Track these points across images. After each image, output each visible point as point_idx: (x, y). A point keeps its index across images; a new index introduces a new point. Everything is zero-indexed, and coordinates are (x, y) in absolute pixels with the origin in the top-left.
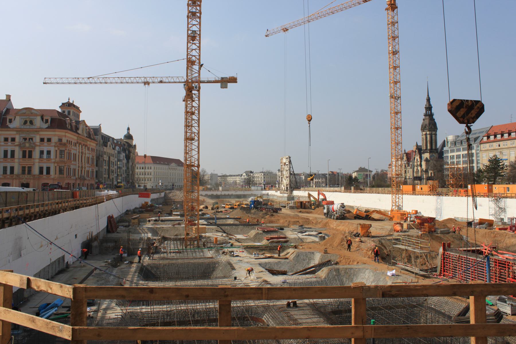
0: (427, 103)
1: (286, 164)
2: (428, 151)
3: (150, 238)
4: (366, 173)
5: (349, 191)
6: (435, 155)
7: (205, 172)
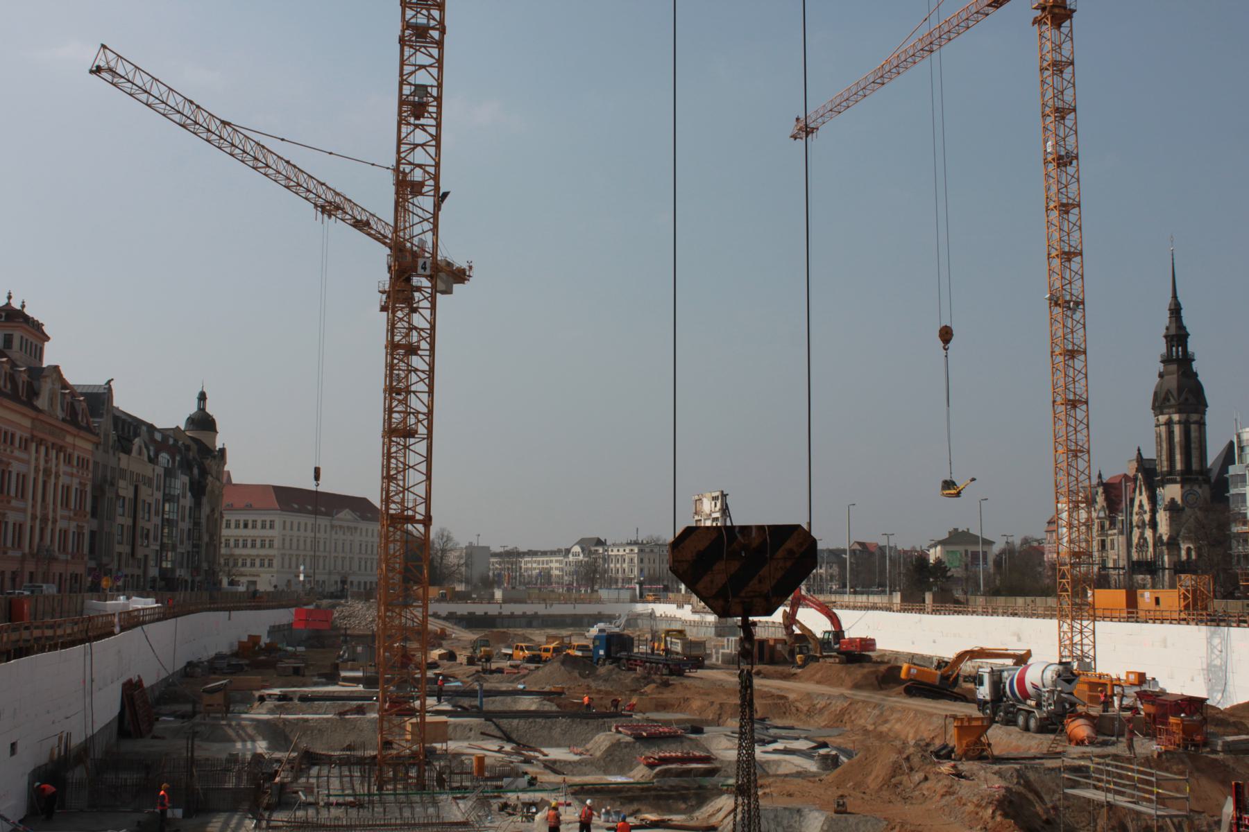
0: (1170, 322)
1: (715, 515)
2: (1178, 478)
3: (261, 755)
4: (971, 548)
5: (917, 606)
6: (1200, 491)
7: (449, 539)
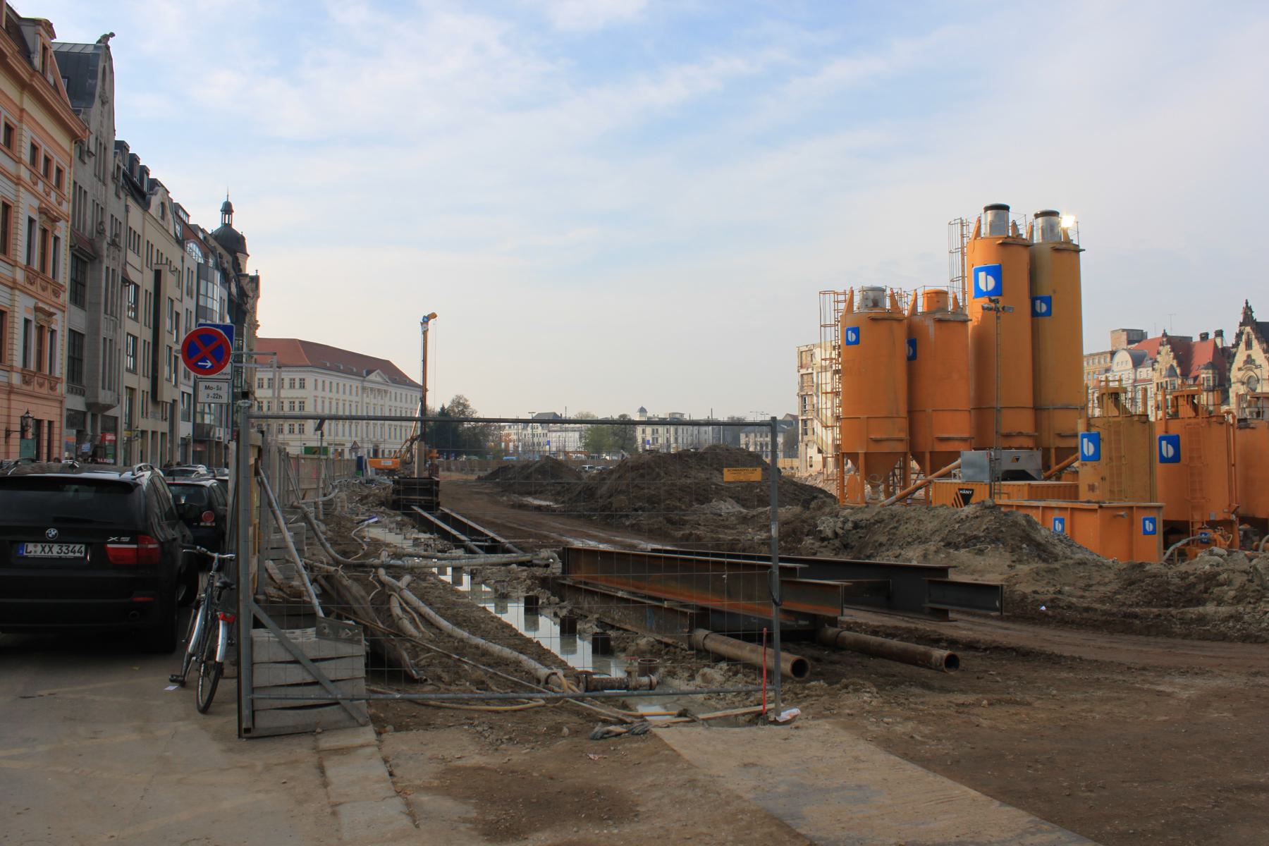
7: (465, 406)
